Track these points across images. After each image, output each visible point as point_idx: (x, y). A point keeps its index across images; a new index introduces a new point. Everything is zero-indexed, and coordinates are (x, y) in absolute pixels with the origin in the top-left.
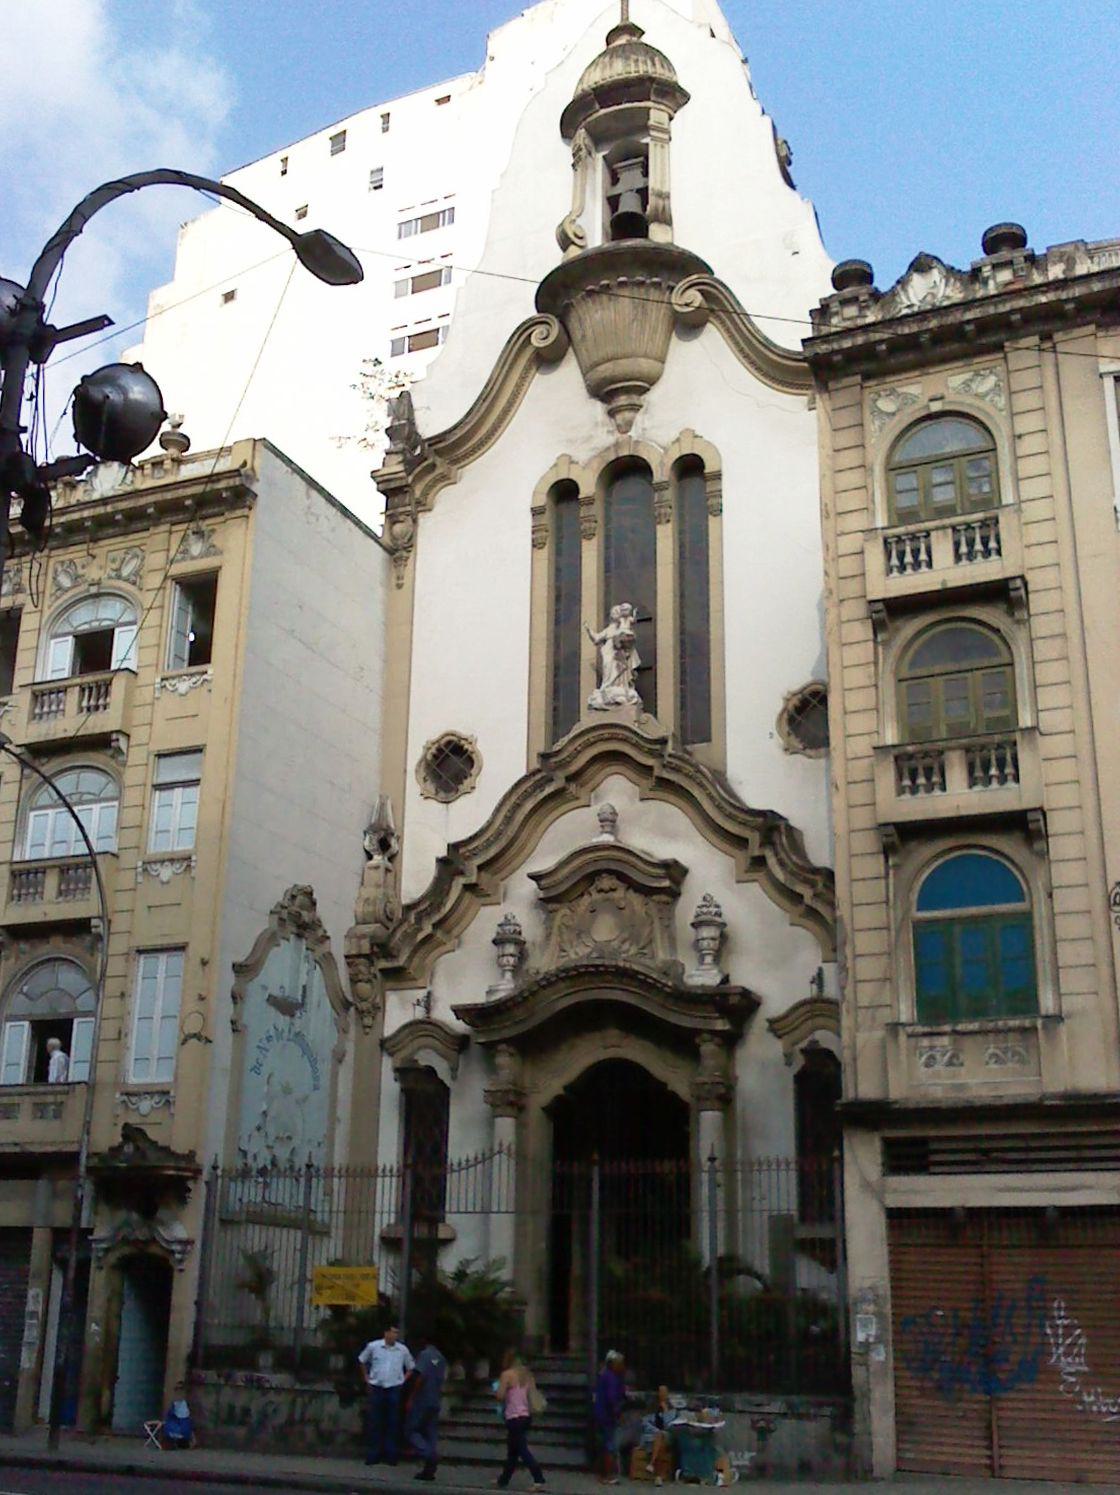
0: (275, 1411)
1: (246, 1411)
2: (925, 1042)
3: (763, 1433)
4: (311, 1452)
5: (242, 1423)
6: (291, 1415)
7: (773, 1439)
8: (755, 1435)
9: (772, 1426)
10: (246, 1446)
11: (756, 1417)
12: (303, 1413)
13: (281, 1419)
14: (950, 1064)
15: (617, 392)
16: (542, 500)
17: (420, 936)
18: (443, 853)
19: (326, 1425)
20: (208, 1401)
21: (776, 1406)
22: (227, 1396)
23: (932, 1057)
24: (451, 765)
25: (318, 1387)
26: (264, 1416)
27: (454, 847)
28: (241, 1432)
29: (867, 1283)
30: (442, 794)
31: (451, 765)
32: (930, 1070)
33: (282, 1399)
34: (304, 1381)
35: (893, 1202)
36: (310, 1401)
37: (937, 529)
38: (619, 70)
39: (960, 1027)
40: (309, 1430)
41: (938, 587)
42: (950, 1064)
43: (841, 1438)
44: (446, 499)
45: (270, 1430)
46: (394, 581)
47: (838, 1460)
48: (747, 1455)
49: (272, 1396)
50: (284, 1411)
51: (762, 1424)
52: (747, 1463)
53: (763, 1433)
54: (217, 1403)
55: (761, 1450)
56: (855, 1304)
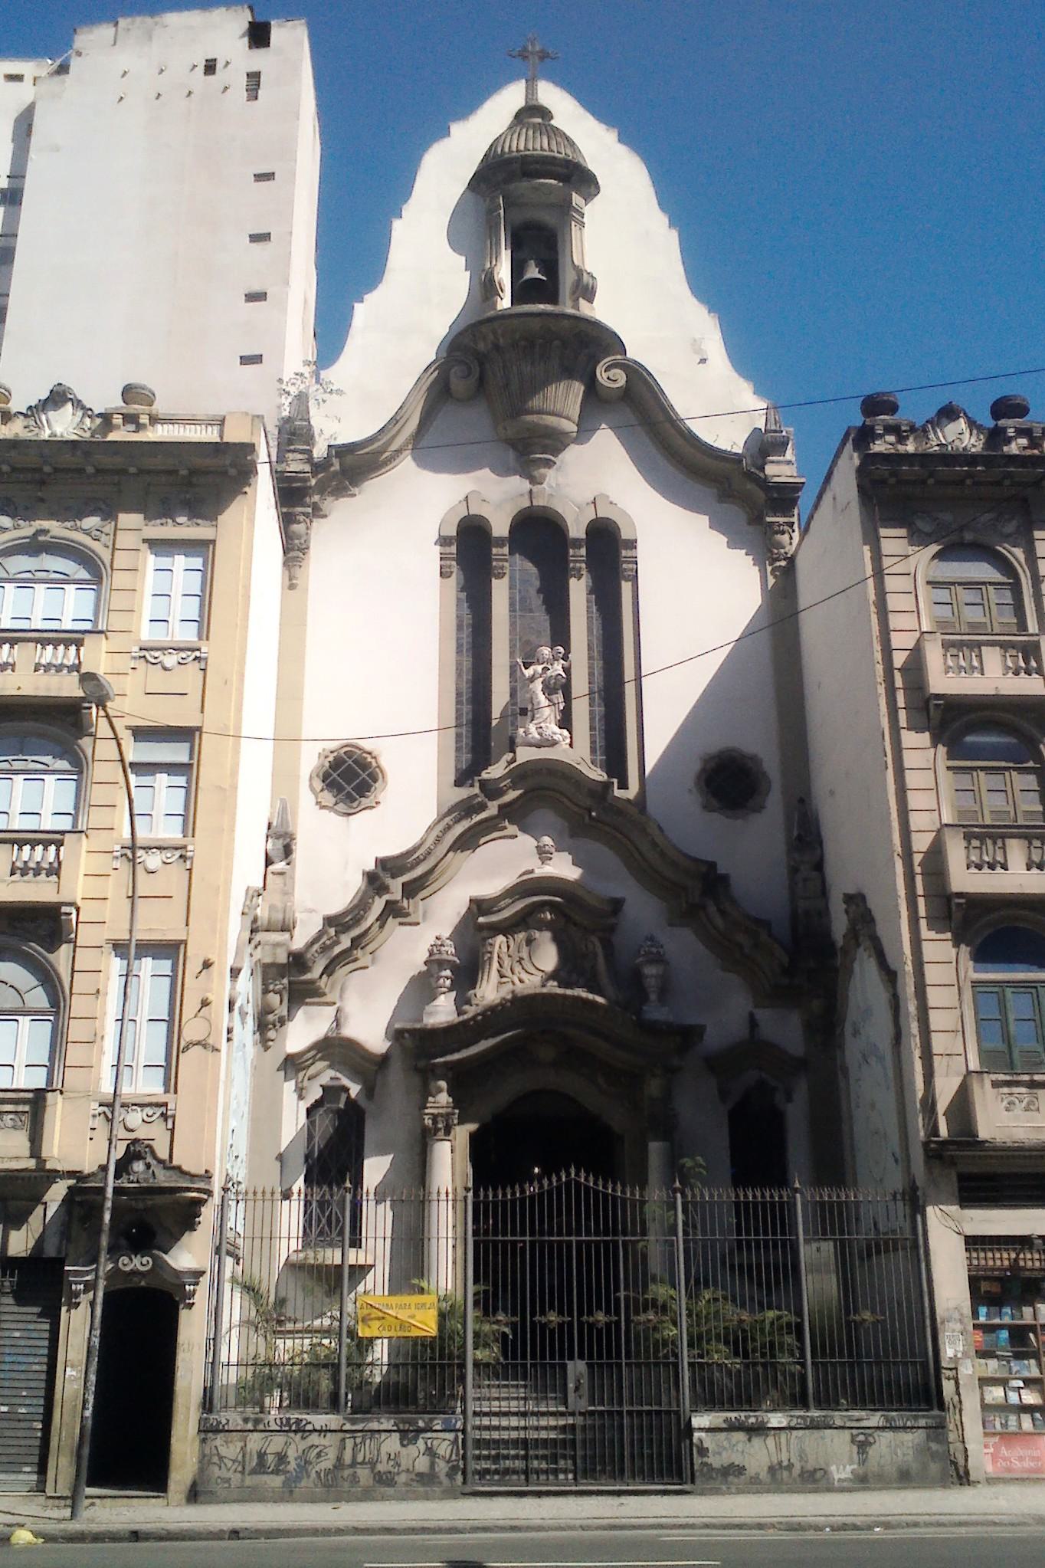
0: (319, 1455)
1: (282, 1458)
2: (1006, 1090)
3: (863, 1446)
4: (366, 1496)
5: (276, 1472)
6: (339, 1459)
8: (855, 1449)
9: (871, 1439)
10: (288, 1495)
11: (855, 1432)
12: (354, 1457)
13: (327, 1464)
14: (1027, 1109)
15: (530, 449)
16: (452, 532)
17: (337, 950)
18: (371, 866)
19: (380, 1467)
20: (230, 1449)
21: (876, 1419)
22: (255, 1442)
24: (350, 778)
25: (375, 1426)
26: (305, 1463)
27: (383, 863)
28: (277, 1481)
29: (952, 1304)
30: (341, 807)
31: (350, 778)
33: (329, 1440)
34: (353, 1422)
35: (971, 1231)
36: (363, 1442)
37: (992, 644)
38: (519, 144)
39: (1036, 1077)
40: (364, 1474)
41: (993, 693)
43: (934, 1446)
44: (340, 510)
45: (313, 1475)
46: (287, 583)
47: (934, 1468)
48: (849, 1468)
49: (314, 1439)
50: (332, 1454)
51: (861, 1438)
52: (850, 1476)
53: (863, 1446)
55: (863, 1462)
56: (943, 1323)
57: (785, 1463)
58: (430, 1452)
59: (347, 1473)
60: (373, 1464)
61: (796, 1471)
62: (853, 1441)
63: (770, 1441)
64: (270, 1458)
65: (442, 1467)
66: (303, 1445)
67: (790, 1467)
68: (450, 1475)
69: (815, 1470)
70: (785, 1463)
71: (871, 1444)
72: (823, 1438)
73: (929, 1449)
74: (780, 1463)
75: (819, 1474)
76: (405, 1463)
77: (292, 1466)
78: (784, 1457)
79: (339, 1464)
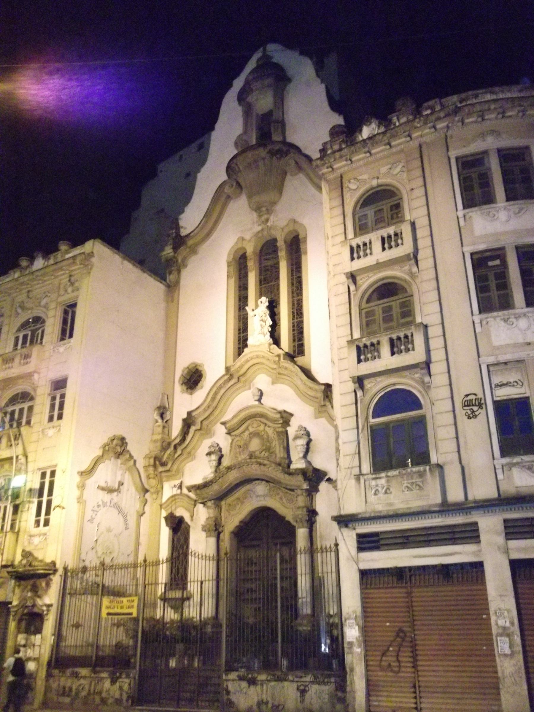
1: (71, 689)
5: (68, 696)
6: (89, 690)
7: (307, 695)
8: (299, 694)
9: (307, 689)
11: (299, 684)
13: (84, 693)
18: (185, 416)
19: (104, 695)
21: (309, 678)
23: (377, 490)
28: (67, 700)
30: (189, 391)
31: (193, 379)
32: (376, 497)
35: (364, 566)
42: (386, 492)
43: (340, 694)
50: (87, 687)
51: (302, 688)
54: (59, 684)
55: (302, 701)
56: (346, 621)
57: (265, 700)
58: (121, 688)
59: (92, 697)
60: (100, 693)
61: (270, 705)
62: (298, 689)
63: (259, 688)
64: (67, 689)
65: (125, 697)
66: (79, 683)
67: (267, 703)
68: (127, 700)
69: (279, 705)
70: (265, 700)
71: (307, 692)
72: (283, 687)
73: (337, 695)
74: (262, 701)
75: (280, 708)
76: (111, 693)
77: (73, 693)
78: (264, 696)
79: (89, 693)
